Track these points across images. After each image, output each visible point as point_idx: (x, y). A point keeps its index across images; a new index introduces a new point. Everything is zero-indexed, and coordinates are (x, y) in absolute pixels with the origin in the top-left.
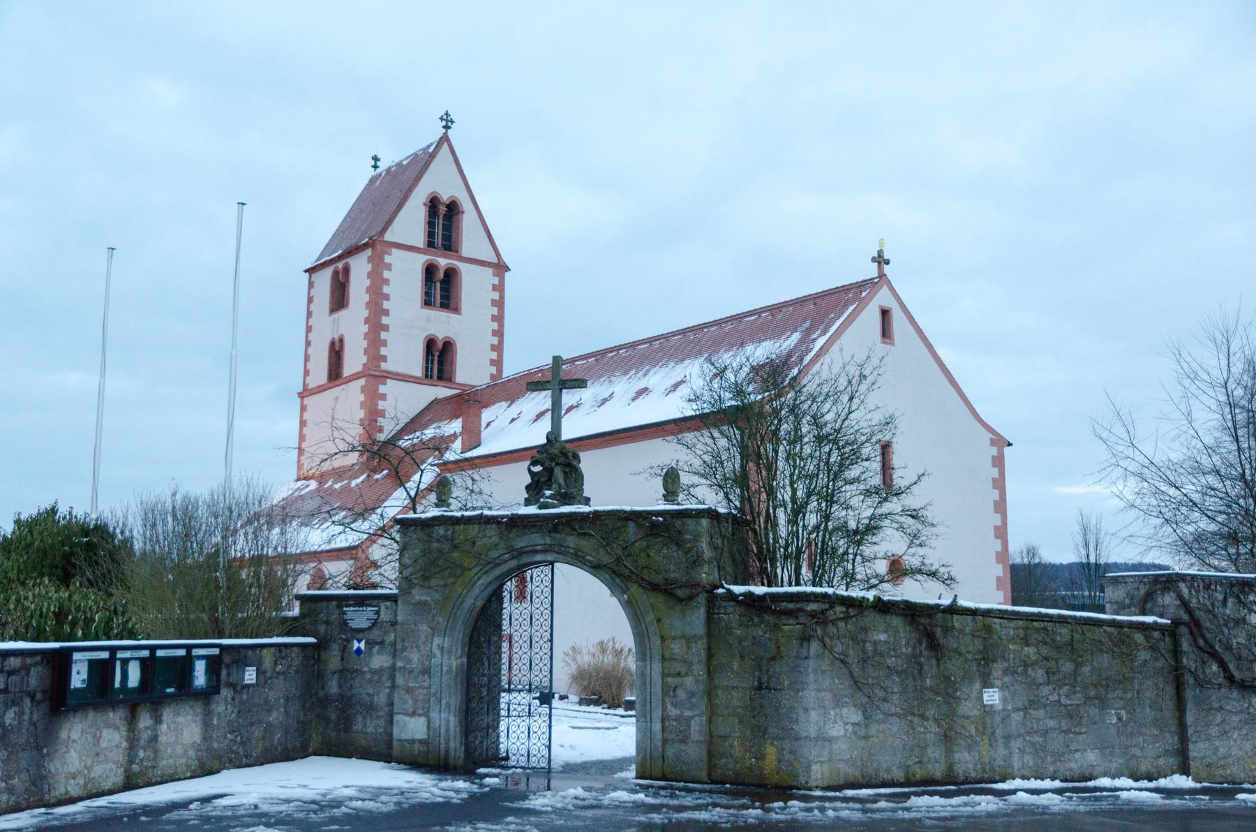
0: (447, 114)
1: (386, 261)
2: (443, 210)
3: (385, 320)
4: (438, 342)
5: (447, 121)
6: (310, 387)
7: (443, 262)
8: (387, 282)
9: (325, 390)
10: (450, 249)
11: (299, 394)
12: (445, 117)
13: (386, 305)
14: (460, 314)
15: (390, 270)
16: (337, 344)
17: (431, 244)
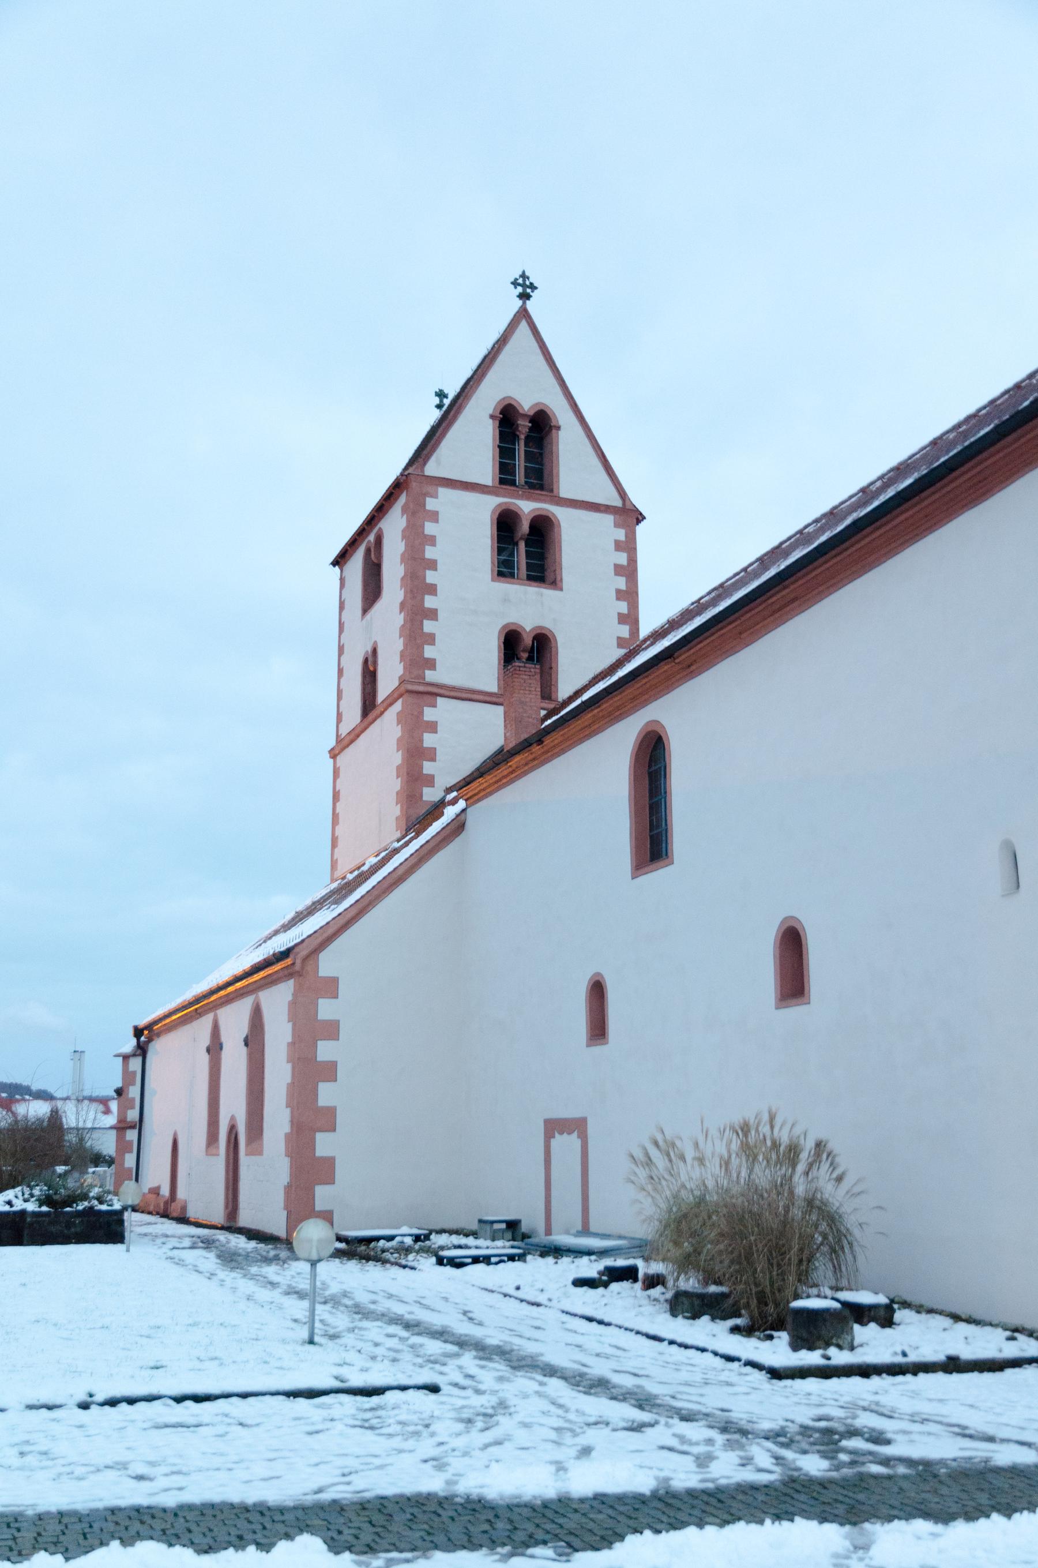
0: (523, 276)
1: (428, 507)
3: (429, 602)
4: (525, 636)
5: (525, 289)
7: (527, 507)
8: (432, 540)
9: (358, 736)
10: (541, 487)
12: (520, 281)
13: (431, 577)
14: (561, 589)
15: (436, 521)
16: (370, 659)
17: (506, 475)
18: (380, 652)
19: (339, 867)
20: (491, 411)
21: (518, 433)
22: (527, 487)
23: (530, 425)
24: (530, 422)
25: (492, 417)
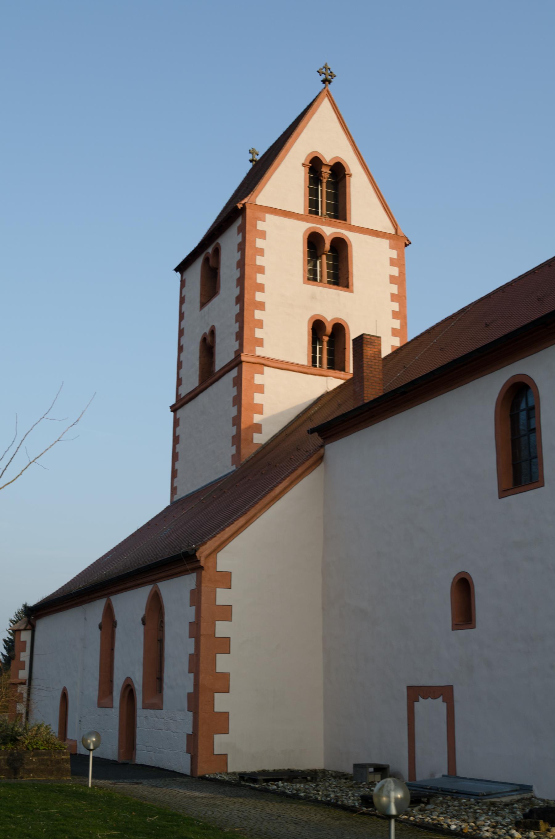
2: (326, 172)
4: (326, 324)
6: (182, 396)
11: (171, 407)
14: (352, 292)
16: (209, 339)
18: (217, 333)
19: (179, 492)
20: (303, 161)
21: (321, 178)
22: (328, 217)
23: (330, 172)
24: (330, 170)
25: (304, 165)
